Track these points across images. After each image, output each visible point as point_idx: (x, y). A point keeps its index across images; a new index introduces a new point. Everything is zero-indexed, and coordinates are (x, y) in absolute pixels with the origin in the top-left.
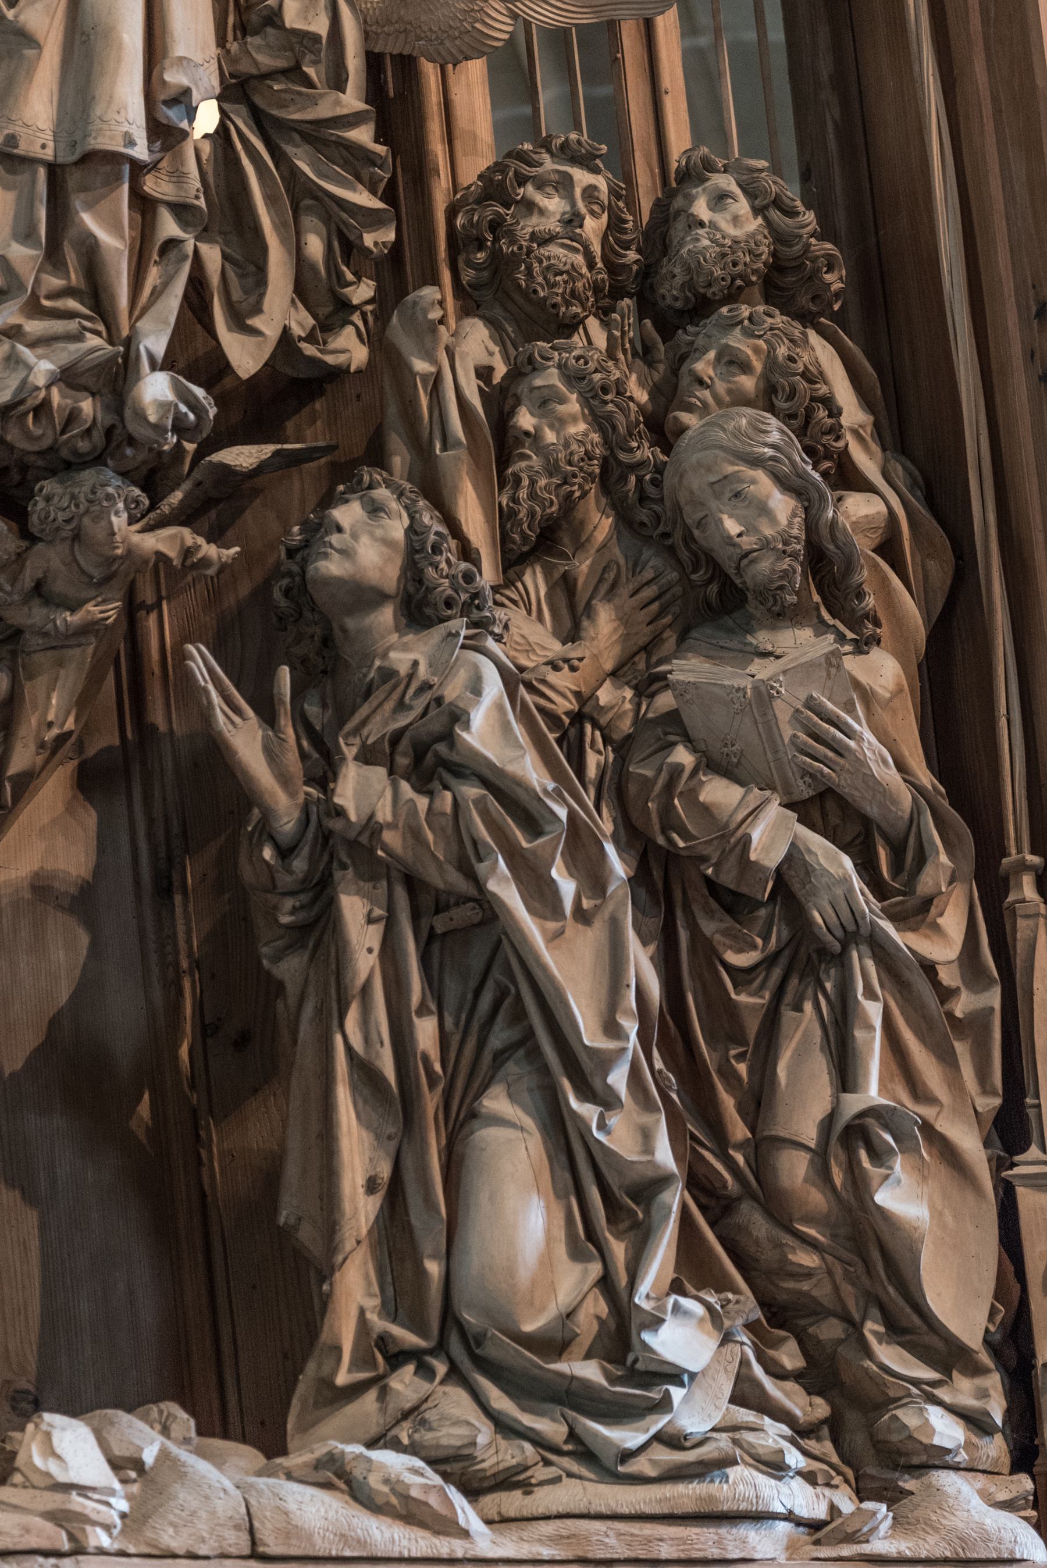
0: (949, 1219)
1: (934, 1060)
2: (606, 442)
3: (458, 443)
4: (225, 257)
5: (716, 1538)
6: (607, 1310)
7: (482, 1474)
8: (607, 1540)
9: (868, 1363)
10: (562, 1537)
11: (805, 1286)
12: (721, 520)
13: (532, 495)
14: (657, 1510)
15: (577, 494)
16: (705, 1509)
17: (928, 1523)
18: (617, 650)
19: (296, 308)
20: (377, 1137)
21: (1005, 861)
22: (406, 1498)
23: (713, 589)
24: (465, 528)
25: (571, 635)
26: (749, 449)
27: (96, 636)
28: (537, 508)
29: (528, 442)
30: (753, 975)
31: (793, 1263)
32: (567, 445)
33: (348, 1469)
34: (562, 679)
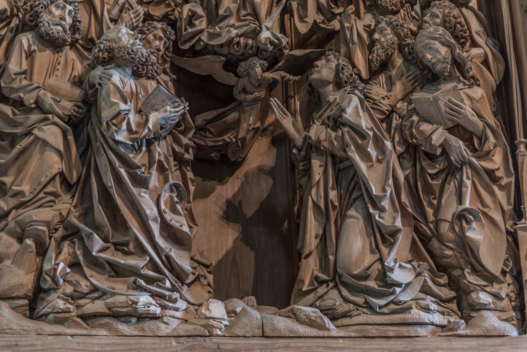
0: (492, 240)
1: (489, 196)
2: (399, 40)
3: (356, 43)
4: (298, 4)
5: (407, 330)
6: (381, 267)
7: (337, 313)
8: (372, 331)
9: (465, 281)
10: (359, 330)
11: (449, 260)
12: (426, 55)
13: (378, 55)
14: (388, 322)
15: (390, 53)
16: (403, 322)
18: (402, 93)
19: (319, 15)
20: (319, 223)
21: (516, 141)
22: (310, 320)
23: (430, 75)
24: (357, 64)
25: (389, 90)
26: (432, 36)
27: (261, 101)
28: (378, 58)
29: (377, 42)
30: (437, 176)
31: (445, 254)
32: (387, 41)
33: (295, 312)
34: (386, 102)
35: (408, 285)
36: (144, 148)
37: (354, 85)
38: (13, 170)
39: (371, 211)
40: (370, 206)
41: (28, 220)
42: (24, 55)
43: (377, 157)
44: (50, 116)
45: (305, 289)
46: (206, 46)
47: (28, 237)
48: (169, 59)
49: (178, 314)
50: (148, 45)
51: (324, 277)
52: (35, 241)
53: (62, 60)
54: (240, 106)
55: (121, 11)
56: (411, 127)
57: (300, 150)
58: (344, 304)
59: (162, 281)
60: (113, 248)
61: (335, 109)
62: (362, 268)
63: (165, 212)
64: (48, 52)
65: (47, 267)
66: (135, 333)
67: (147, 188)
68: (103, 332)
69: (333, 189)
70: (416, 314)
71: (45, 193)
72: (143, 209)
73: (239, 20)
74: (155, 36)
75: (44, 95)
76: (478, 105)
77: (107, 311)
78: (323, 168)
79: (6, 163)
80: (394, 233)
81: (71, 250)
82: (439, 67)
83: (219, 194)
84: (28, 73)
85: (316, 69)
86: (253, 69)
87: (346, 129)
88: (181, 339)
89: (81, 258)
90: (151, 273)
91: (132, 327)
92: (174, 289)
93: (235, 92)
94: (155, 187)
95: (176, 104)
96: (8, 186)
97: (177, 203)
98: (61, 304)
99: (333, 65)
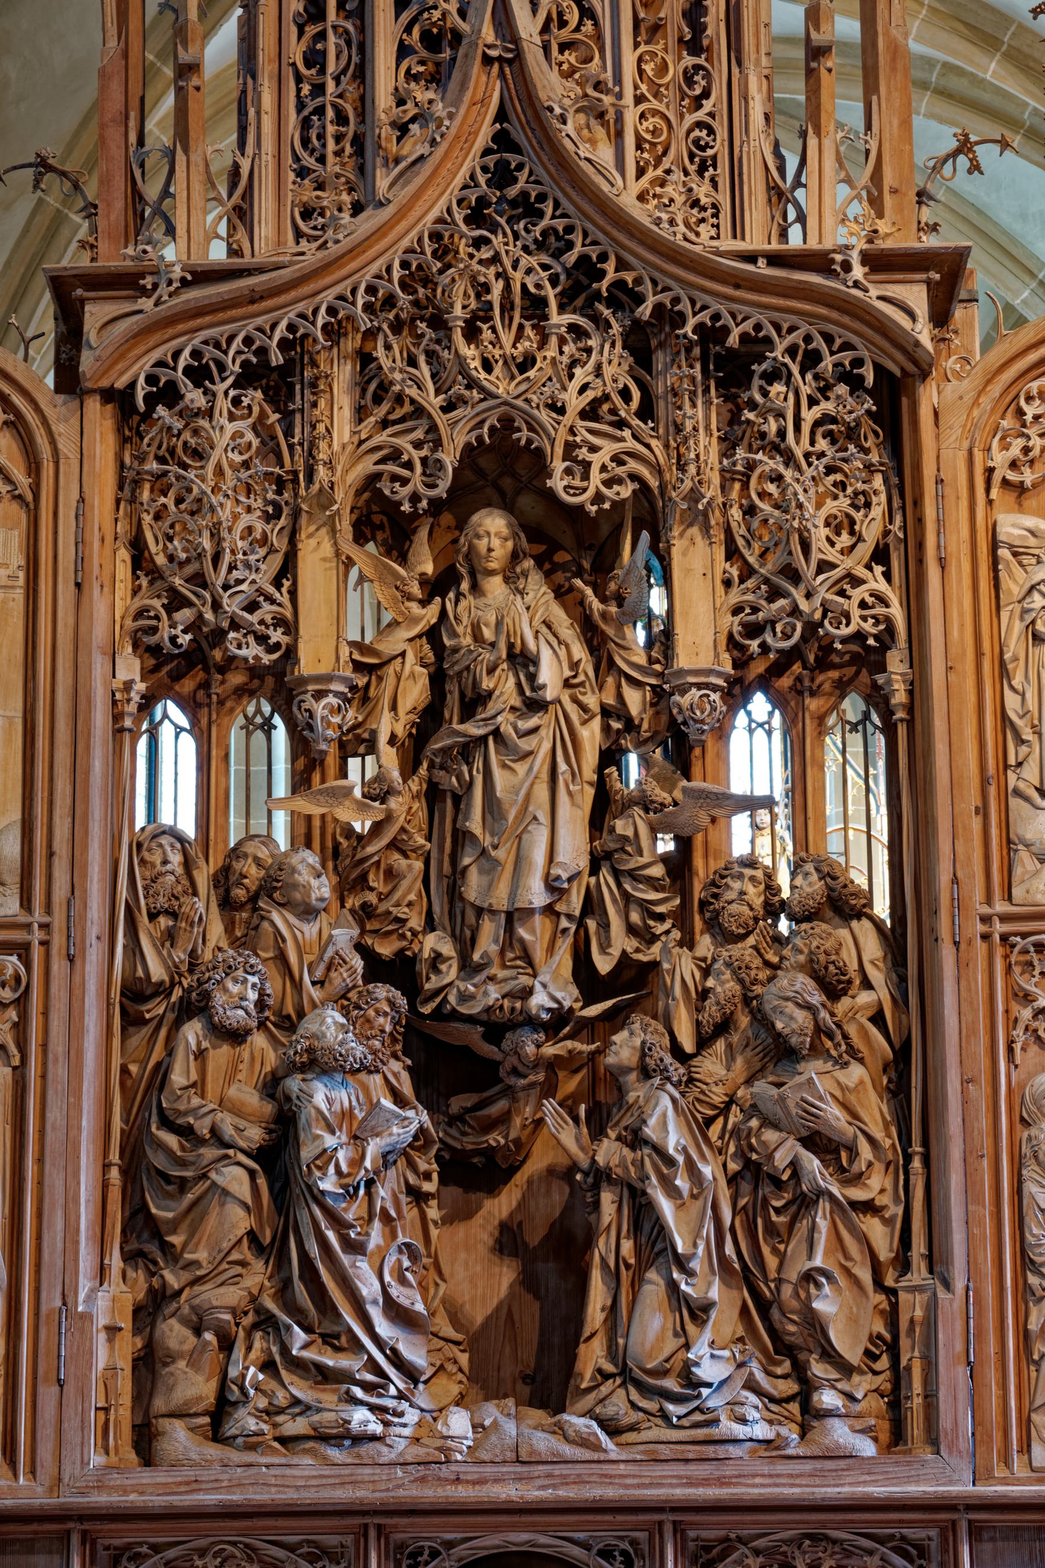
17: (814, 1441)
34: (719, 1090)
35: (723, 1383)
36: (362, 1192)
37: (666, 1074)
38: (184, 1226)
39: (675, 1275)
40: (674, 1268)
41: (206, 1307)
42: (192, 1057)
43: (691, 1190)
44: (231, 1152)
45: (583, 1386)
46: (454, 1010)
47: (208, 1329)
48: (400, 1038)
49: (407, 1432)
50: (367, 1025)
51: (609, 1368)
52: (217, 1335)
53: (246, 1055)
54: (509, 1092)
55: (328, 969)
56: (749, 1135)
57: (586, 1174)
58: (631, 1412)
59: (384, 1387)
60: (320, 1341)
61: (636, 1114)
62: (661, 1358)
63: (389, 1285)
64: (225, 1049)
65: (233, 1372)
66: (349, 1461)
67: (365, 1255)
68: (308, 1460)
69: (628, 1238)
70: (728, 1427)
71: (229, 1263)
72: (357, 1289)
73: (504, 966)
74: (377, 1012)
75: (222, 1120)
76: (852, 1099)
77: (312, 1433)
78: (616, 1205)
79: (175, 1219)
80: (707, 1307)
81: (265, 1345)
82: (794, 1040)
83: (489, 1212)
84: (199, 1087)
85: (613, 1048)
86: (522, 1048)
87: (647, 1151)
88: (409, 1467)
89: (278, 1358)
90: (370, 1377)
91: (345, 1452)
92: (401, 1396)
94: (378, 1247)
95: (406, 1123)
96: (179, 1249)
97: (407, 1269)
98: (252, 1424)
99: (638, 1042)
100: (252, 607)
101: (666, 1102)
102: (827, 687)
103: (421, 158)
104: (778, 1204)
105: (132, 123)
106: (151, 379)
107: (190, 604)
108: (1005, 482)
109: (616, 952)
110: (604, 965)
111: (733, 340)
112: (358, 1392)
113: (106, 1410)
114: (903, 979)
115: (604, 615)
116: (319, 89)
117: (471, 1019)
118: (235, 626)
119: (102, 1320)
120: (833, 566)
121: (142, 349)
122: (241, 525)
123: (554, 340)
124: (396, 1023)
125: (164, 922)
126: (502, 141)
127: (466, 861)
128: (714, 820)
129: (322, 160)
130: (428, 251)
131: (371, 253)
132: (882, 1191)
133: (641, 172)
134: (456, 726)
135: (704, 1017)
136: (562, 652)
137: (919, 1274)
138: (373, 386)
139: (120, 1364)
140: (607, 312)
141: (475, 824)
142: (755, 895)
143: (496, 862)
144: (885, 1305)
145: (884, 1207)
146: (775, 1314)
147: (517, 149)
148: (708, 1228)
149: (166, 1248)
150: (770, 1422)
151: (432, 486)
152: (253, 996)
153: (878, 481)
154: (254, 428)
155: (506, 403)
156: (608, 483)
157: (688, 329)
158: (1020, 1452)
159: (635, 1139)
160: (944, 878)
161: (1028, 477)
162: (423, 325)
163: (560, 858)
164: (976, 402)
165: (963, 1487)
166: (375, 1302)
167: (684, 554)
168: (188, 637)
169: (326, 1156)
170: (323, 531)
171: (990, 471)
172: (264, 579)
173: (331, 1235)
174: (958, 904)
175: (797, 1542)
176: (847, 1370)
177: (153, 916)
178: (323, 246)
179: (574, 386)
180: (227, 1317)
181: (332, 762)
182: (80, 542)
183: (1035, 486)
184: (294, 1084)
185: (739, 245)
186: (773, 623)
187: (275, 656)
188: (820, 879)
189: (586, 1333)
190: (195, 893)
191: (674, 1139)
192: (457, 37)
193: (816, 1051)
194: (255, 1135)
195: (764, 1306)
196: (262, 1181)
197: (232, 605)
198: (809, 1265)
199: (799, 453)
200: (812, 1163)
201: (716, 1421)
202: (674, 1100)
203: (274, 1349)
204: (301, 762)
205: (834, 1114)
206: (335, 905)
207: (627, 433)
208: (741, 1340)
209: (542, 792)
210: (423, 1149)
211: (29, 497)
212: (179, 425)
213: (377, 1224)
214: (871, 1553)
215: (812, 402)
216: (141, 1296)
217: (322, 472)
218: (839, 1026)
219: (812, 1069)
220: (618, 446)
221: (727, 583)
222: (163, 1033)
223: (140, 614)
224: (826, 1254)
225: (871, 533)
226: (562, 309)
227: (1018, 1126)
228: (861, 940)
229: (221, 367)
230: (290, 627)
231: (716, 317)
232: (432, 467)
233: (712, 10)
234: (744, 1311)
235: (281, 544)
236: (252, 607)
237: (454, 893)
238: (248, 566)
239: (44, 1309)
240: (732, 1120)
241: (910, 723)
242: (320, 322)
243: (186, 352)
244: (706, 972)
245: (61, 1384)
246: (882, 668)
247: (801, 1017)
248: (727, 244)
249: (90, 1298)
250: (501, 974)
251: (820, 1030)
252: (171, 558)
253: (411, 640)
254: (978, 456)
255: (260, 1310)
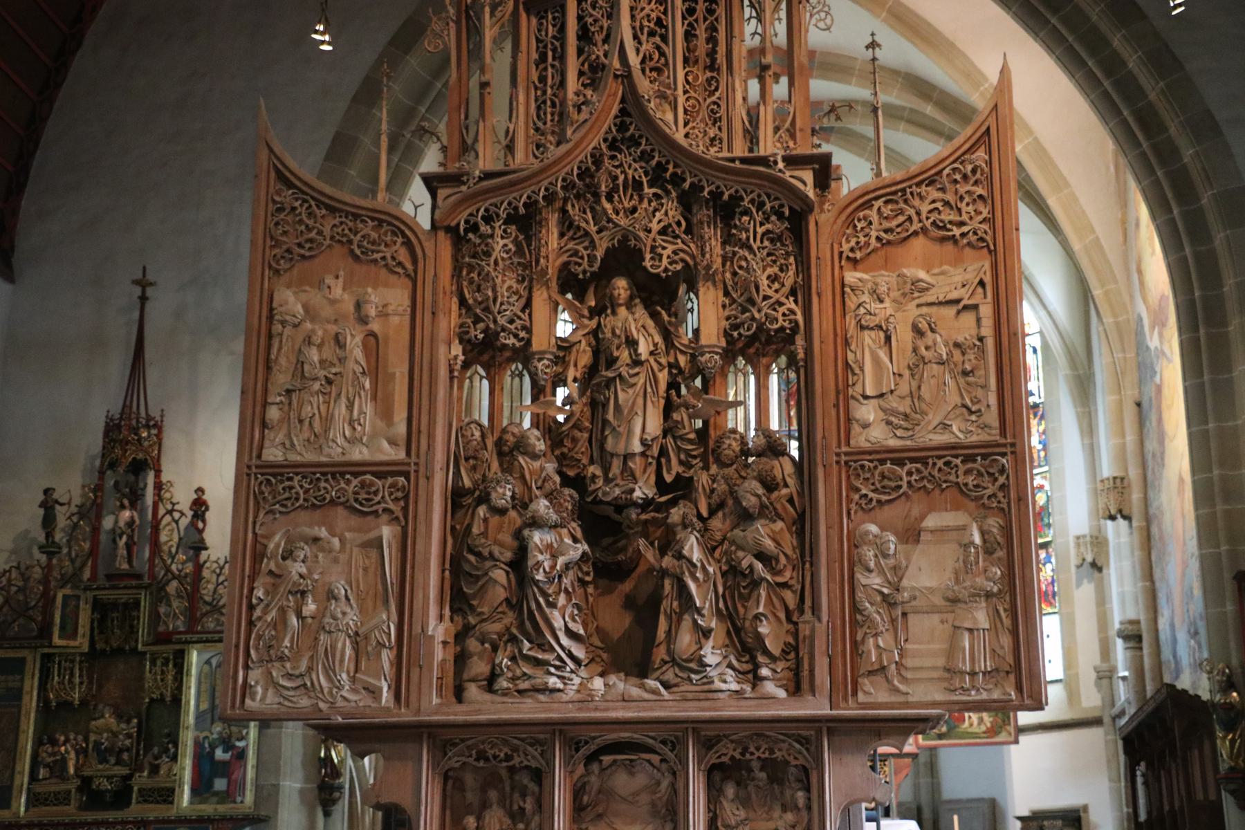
34: (719, 534)
35: (717, 665)
36: (556, 580)
46: (601, 500)
49: (575, 688)
51: (667, 658)
52: (491, 644)
53: (507, 521)
55: (544, 482)
57: (658, 572)
59: (565, 668)
64: (497, 517)
65: (497, 661)
68: (529, 700)
70: (718, 685)
73: (623, 480)
74: (565, 500)
76: (778, 537)
84: (484, 534)
87: (684, 561)
90: (558, 663)
92: (572, 671)
93: (623, 527)
98: (505, 684)
100: (511, 322)
101: (693, 539)
102: (771, 352)
103: (586, 121)
104: (744, 584)
105: (462, 110)
106: (467, 222)
107: (483, 321)
108: (848, 258)
109: (674, 473)
110: (669, 478)
111: (726, 197)
112: (552, 670)
113: (442, 678)
114: (802, 483)
115: (669, 322)
116: (545, 92)
117: (608, 503)
118: (503, 330)
119: (441, 639)
120: (771, 297)
121: (462, 208)
122: (506, 286)
123: (646, 201)
124: (574, 506)
125: (472, 462)
126: (623, 112)
127: (607, 433)
128: (718, 413)
129: (545, 123)
130: (590, 162)
131: (563, 164)
132: (791, 578)
133: (686, 124)
134: (604, 373)
135: (712, 501)
136: (650, 339)
137: (808, 615)
138: (567, 223)
139: (448, 658)
140: (669, 187)
141: (610, 416)
142: (736, 446)
143: (619, 433)
144: (793, 629)
145: (793, 586)
146: (743, 634)
147: (629, 115)
148: (711, 595)
149: (472, 608)
150: (738, 683)
151: (592, 266)
152: (509, 494)
153: (792, 259)
154: (512, 242)
155: (624, 229)
156: (670, 263)
157: (705, 193)
158: (852, 695)
159: (679, 556)
160: (819, 435)
161: (858, 255)
162: (589, 196)
163: (648, 430)
164: (835, 222)
165: (826, 711)
166: (560, 629)
167: (705, 294)
168: (482, 335)
169: (539, 564)
170: (544, 288)
171: (841, 253)
172: (517, 309)
173: (541, 600)
174: (826, 447)
175: (750, 737)
176: (774, 659)
177: (467, 459)
178: (542, 161)
179: (655, 220)
180: (495, 637)
181: (548, 390)
182: (434, 294)
183: (861, 259)
184: (526, 532)
185: (729, 155)
186: (743, 324)
187: (522, 343)
188: (765, 437)
189: (656, 643)
190: (486, 449)
191: (696, 555)
192: (604, 66)
193: (761, 515)
194: (508, 555)
195: (738, 631)
196: (512, 576)
197: (502, 321)
198: (756, 612)
199: (755, 247)
200: (759, 566)
201: (712, 682)
202: (697, 539)
203: (516, 651)
204: (536, 390)
205: (768, 543)
206: (549, 453)
207: (679, 241)
208: (727, 646)
209: (640, 401)
210: (586, 562)
211: (413, 274)
212: (478, 241)
213: (562, 595)
214: (784, 741)
215: (762, 224)
216: (460, 628)
217: (542, 260)
218: (771, 504)
219: (759, 525)
220: (675, 247)
221: (724, 306)
222: (470, 511)
223: (461, 326)
224: (765, 606)
225: (789, 283)
226: (650, 186)
227: (853, 548)
228: (784, 465)
229: (498, 215)
230: (528, 330)
231: (718, 187)
232: (592, 258)
233: (720, 52)
234: (728, 633)
235: (525, 294)
236: (511, 322)
237: (602, 448)
238: (509, 303)
239: (413, 633)
240: (725, 547)
241: (806, 367)
242: (541, 195)
243: (482, 210)
244: (714, 481)
245: (421, 667)
246: (793, 343)
247: (754, 500)
248: (725, 154)
249: (434, 629)
250: (622, 483)
251: (763, 506)
252: (475, 300)
253: (584, 335)
254: (836, 246)
255: (511, 634)
